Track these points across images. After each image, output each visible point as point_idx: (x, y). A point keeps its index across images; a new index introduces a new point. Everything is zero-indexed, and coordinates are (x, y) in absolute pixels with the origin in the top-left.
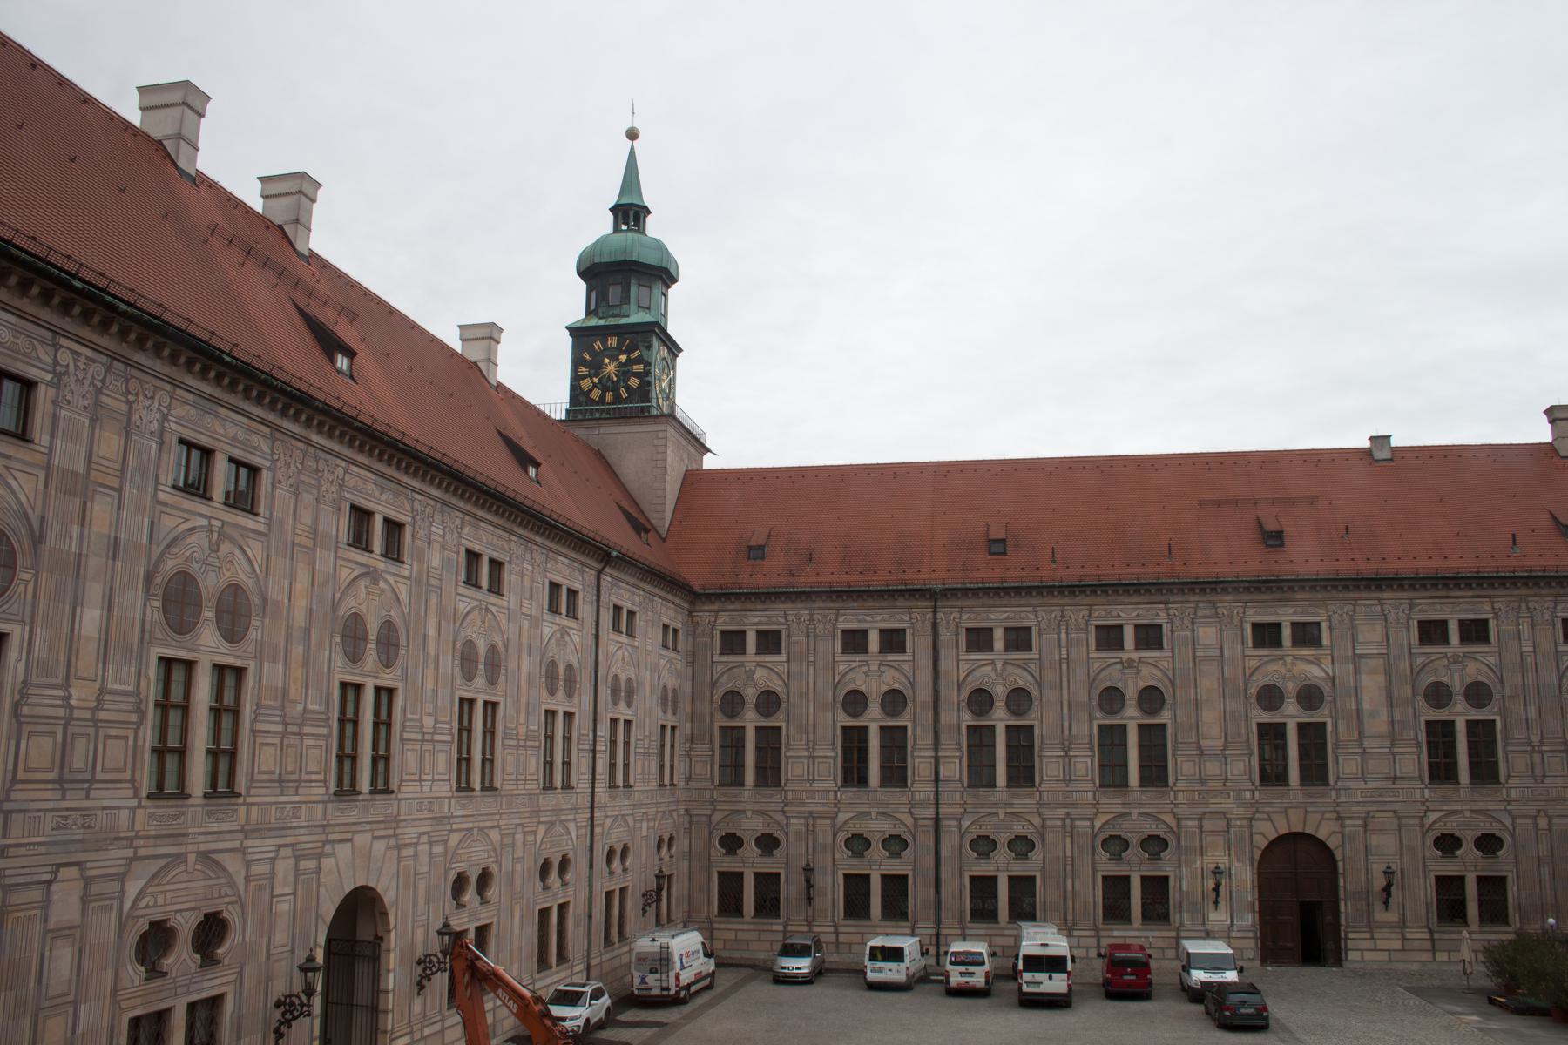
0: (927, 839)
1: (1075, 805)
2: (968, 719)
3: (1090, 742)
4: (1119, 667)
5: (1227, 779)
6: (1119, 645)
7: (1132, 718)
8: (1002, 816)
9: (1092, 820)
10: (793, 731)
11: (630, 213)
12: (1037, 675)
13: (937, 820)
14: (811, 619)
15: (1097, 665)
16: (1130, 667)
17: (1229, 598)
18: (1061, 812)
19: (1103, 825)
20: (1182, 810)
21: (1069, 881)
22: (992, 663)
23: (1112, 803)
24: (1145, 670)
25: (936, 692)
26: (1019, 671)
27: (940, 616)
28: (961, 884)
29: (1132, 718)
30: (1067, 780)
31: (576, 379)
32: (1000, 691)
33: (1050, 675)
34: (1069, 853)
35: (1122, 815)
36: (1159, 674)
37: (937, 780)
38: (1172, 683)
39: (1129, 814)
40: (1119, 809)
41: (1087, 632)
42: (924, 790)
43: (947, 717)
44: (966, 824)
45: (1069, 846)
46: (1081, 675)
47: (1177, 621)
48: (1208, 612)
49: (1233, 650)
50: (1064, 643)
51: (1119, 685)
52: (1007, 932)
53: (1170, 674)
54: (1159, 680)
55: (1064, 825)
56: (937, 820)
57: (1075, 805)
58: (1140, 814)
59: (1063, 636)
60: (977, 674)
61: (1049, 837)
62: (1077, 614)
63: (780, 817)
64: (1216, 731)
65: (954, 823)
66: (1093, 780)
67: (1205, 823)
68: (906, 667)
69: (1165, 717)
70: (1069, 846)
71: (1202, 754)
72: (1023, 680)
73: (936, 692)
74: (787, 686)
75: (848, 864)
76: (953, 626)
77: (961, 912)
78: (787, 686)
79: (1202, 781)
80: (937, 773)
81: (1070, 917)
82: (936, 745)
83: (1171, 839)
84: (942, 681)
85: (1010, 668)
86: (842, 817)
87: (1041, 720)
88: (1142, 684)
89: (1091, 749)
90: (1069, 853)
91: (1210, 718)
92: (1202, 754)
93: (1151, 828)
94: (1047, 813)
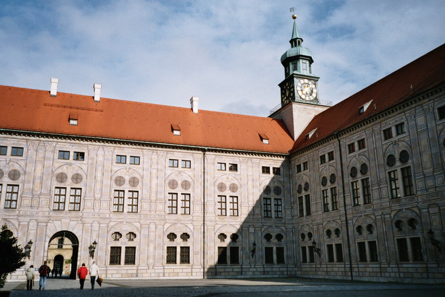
0: (344, 229)
1: (384, 209)
2: (351, 180)
3: (386, 181)
4: (392, 145)
5: (436, 187)
6: (390, 136)
7: (398, 166)
8: (363, 216)
9: (390, 214)
10: (312, 196)
11: (295, 42)
12: (368, 157)
13: (347, 221)
14: (313, 155)
15: (385, 147)
16: (395, 144)
17: (427, 100)
18: (380, 212)
19: (394, 215)
20: (420, 205)
21: (386, 242)
22: (355, 156)
23: (396, 207)
24: (401, 144)
25: (342, 172)
26: (363, 157)
27: (341, 143)
28: (355, 246)
29: (398, 166)
30: (381, 198)
31: (282, 99)
32: (358, 167)
33: (372, 156)
34: (385, 230)
35: (400, 210)
36: (405, 144)
37: (345, 206)
38: (411, 147)
39: (402, 209)
40: (398, 208)
41: (381, 134)
42: (342, 209)
43: (346, 181)
44: (354, 221)
45: (384, 227)
46: (381, 153)
47: (409, 118)
48: (420, 110)
49: (432, 125)
50: (374, 142)
51: (393, 153)
52: (370, 266)
53: (409, 143)
54: (406, 147)
55: (382, 218)
56: (347, 221)
57: (384, 209)
58: (406, 209)
59: (374, 138)
60: (352, 162)
61: (378, 223)
62: (377, 128)
63: (311, 226)
64: (429, 165)
65: (351, 221)
66: (388, 196)
67: (430, 210)
68: (335, 165)
69: (410, 163)
70: (384, 227)
71: (425, 177)
72: (364, 160)
73: (342, 172)
74: (310, 180)
75: (327, 241)
76: (344, 144)
77: (357, 258)
78: (310, 180)
79: (427, 190)
80: (345, 202)
81: (388, 259)
82: (344, 193)
83: (418, 219)
84: (344, 167)
85: (360, 156)
86: (325, 223)
87: (371, 176)
88: (400, 150)
89: (387, 183)
90: (385, 230)
91: (426, 158)
92: (425, 177)
93: (410, 215)
94: (376, 214)
